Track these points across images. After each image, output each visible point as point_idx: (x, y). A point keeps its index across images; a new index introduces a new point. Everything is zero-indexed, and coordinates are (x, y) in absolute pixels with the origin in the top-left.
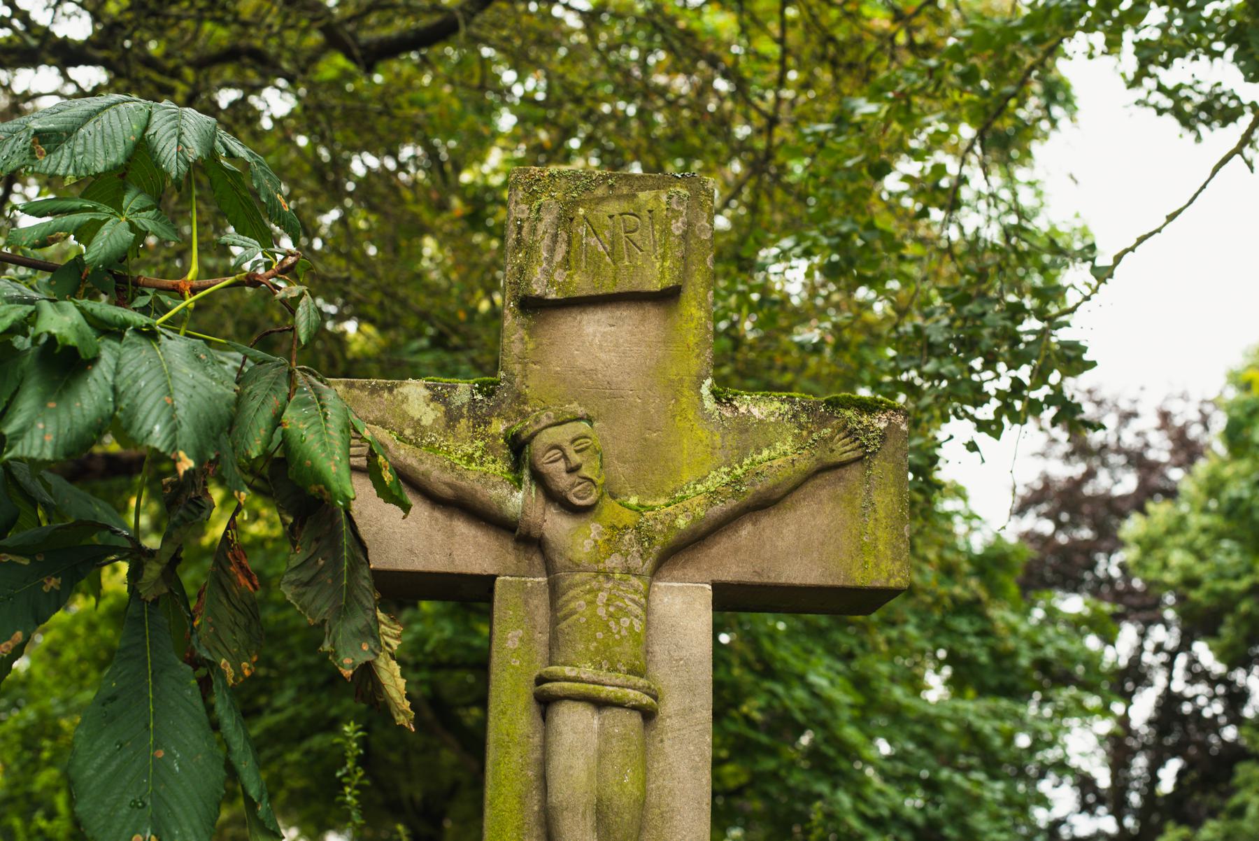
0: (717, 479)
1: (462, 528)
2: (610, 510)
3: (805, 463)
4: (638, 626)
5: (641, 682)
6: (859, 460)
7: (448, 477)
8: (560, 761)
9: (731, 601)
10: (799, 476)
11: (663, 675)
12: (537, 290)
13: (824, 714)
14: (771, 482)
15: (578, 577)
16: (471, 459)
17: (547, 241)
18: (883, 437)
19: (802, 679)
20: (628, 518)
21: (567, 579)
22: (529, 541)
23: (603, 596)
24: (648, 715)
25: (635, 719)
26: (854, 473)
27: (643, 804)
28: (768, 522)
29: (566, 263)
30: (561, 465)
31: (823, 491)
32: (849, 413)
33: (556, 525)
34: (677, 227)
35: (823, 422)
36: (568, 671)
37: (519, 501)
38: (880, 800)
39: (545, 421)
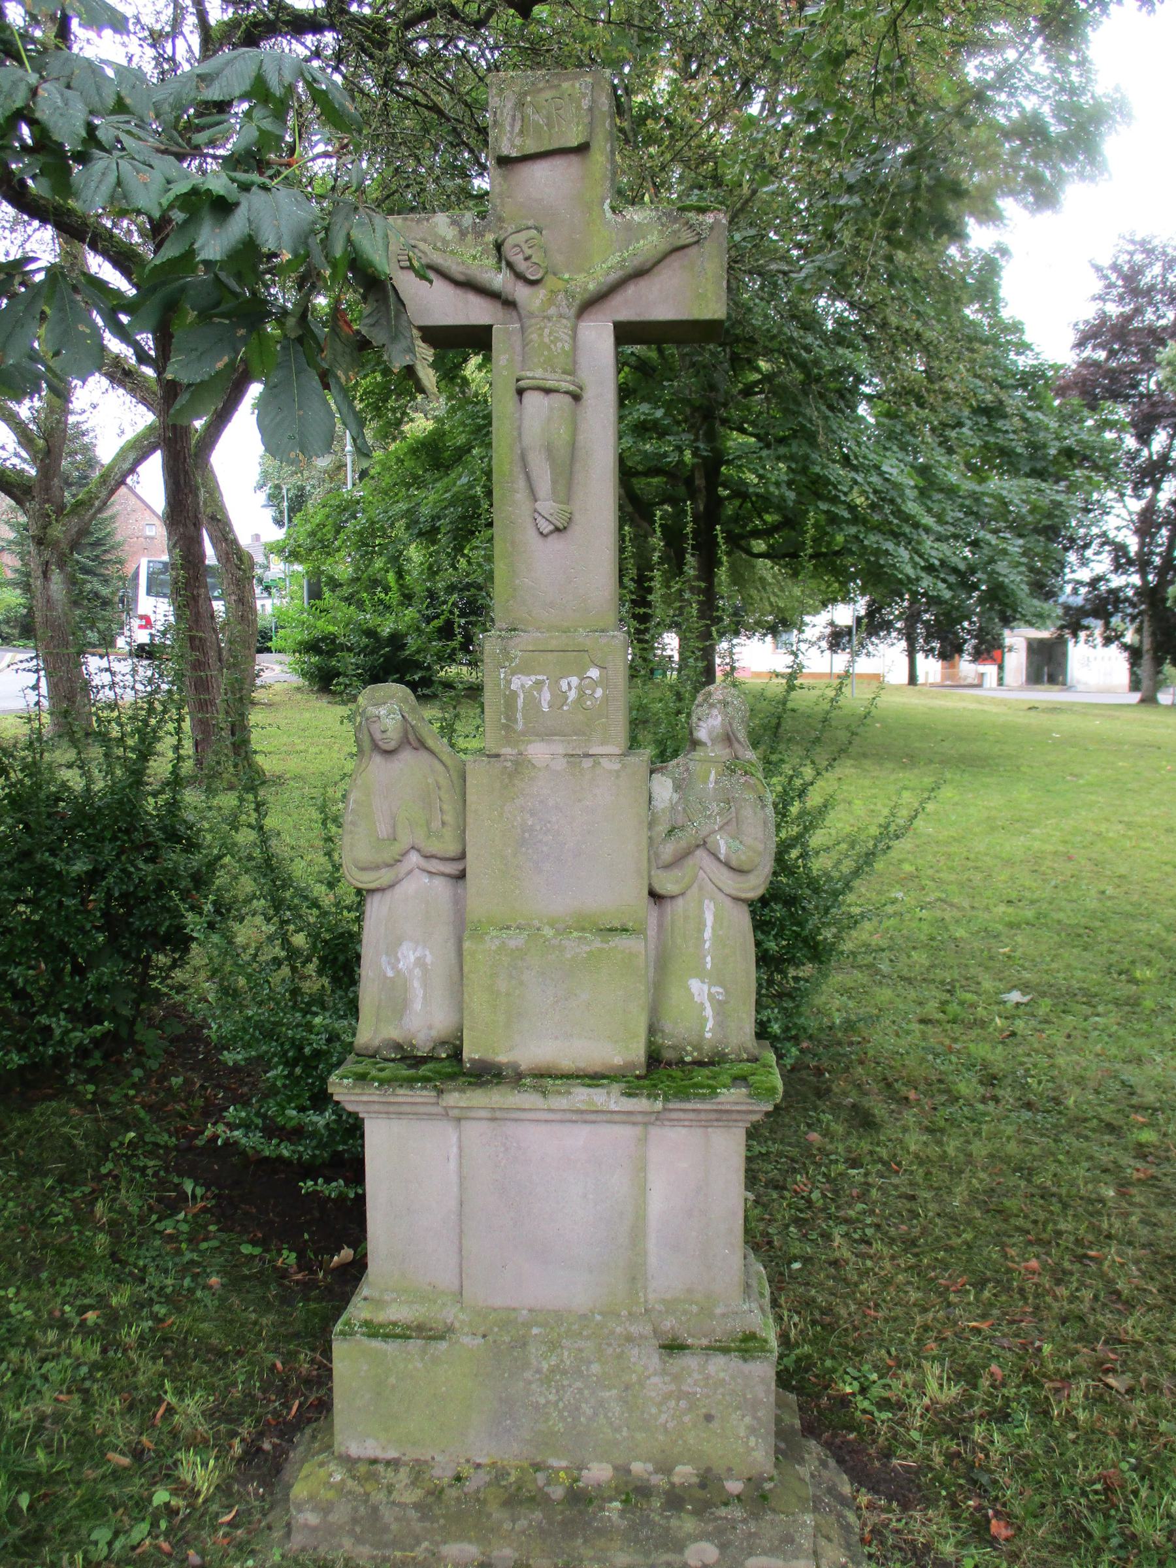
0: (614, 259)
1: (474, 299)
2: (550, 281)
3: (664, 246)
4: (567, 347)
5: (569, 378)
6: (697, 242)
7: (461, 268)
8: (527, 423)
10: (660, 255)
11: (586, 376)
12: (505, 151)
13: (893, 494)
14: (641, 259)
15: (533, 321)
16: (475, 258)
17: (509, 119)
18: (712, 228)
19: (877, 468)
20: (561, 285)
21: (527, 322)
22: (509, 304)
23: (547, 331)
24: (576, 398)
25: (568, 399)
26: (694, 250)
27: (573, 445)
28: (643, 284)
29: (521, 132)
30: (521, 257)
31: (675, 261)
32: (690, 215)
33: (521, 293)
34: (585, 104)
35: (676, 220)
36: (529, 374)
37: (499, 280)
38: (934, 553)
39: (510, 231)
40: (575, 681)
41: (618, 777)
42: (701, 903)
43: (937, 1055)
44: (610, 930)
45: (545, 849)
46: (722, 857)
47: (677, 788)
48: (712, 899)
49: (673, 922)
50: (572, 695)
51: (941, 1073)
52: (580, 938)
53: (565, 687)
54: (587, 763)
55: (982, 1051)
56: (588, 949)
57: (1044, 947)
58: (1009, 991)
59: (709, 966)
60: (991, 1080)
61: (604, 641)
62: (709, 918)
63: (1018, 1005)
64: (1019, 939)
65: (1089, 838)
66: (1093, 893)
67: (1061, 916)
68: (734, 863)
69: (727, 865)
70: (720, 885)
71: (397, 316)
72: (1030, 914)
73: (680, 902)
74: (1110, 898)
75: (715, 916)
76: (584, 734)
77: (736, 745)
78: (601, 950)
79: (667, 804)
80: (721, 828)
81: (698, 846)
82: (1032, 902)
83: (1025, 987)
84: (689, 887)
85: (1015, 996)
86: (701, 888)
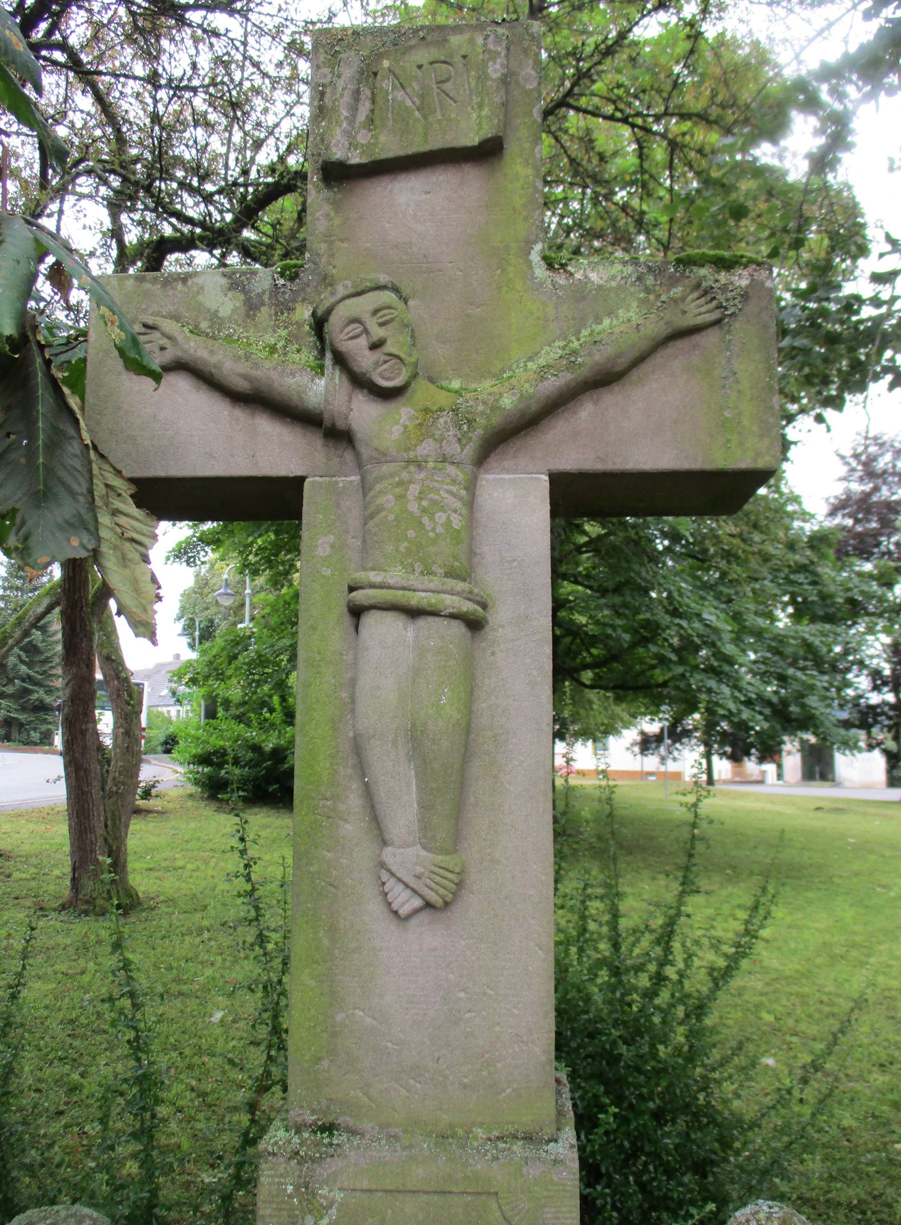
0: (551, 354)
1: (266, 426)
2: (422, 392)
3: (654, 328)
4: (457, 522)
5: (460, 586)
6: (717, 322)
7: (243, 367)
8: (366, 681)
9: (576, 498)
10: (645, 345)
11: (493, 578)
12: (337, 154)
13: (714, 637)
14: (611, 350)
15: (385, 469)
16: (273, 349)
17: (347, 98)
18: (745, 296)
19: (699, 615)
20: (443, 399)
21: (374, 471)
22: (339, 436)
23: (414, 489)
24: (474, 625)
25: (458, 629)
26: (711, 338)
27: (467, 728)
28: (611, 400)
29: (371, 120)
30: (363, 342)
31: (675, 359)
32: (703, 272)
33: (363, 414)
34: (495, 70)
35: (673, 282)
36: (375, 577)
37: (320, 389)
38: (750, 688)
39: (341, 291)
61: (533, 1171)
71: (55, 444)
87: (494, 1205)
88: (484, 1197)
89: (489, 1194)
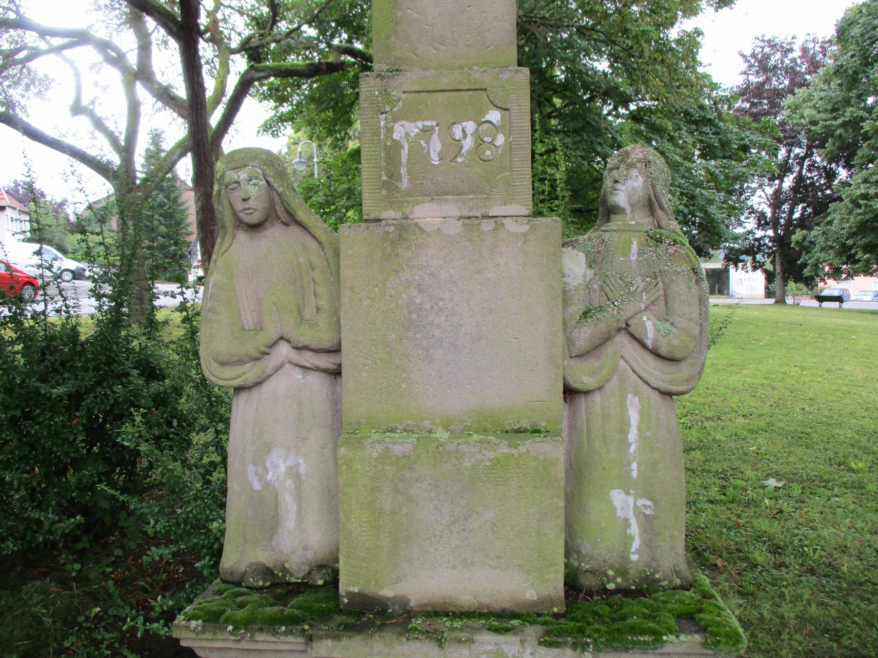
40: (470, 126)
41: (526, 242)
42: (623, 398)
43: (729, 529)
44: (519, 431)
45: (437, 333)
46: (649, 343)
47: (591, 263)
48: (636, 394)
49: (588, 419)
50: (468, 144)
51: (737, 543)
52: (482, 442)
53: (458, 134)
54: (487, 226)
55: (763, 524)
56: (491, 455)
57: (780, 447)
58: (767, 477)
59: (634, 474)
60: (776, 549)
62: (634, 416)
63: (777, 489)
64: (760, 440)
65: (780, 376)
66: (797, 409)
67: (782, 424)
68: (664, 351)
69: (656, 353)
70: (645, 376)
72: (762, 424)
73: (597, 397)
74: (810, 413)
75: (641, 413)
76: (482, 192)
77: (660, 213)
78: (508, 457)
79: (580, 281)
80: (646, 308)
81: (619, 330)
82: (760, 416)
83: (777, 476)
84: (608, 380)
85: (772, 482)
86: (622, 381)
87: (485, 96)
88: (480, 92)
89: (481, 89)
